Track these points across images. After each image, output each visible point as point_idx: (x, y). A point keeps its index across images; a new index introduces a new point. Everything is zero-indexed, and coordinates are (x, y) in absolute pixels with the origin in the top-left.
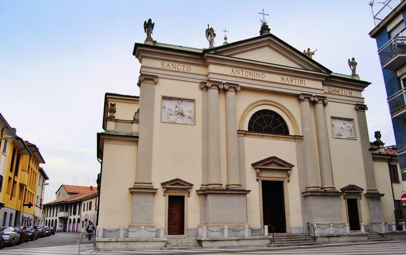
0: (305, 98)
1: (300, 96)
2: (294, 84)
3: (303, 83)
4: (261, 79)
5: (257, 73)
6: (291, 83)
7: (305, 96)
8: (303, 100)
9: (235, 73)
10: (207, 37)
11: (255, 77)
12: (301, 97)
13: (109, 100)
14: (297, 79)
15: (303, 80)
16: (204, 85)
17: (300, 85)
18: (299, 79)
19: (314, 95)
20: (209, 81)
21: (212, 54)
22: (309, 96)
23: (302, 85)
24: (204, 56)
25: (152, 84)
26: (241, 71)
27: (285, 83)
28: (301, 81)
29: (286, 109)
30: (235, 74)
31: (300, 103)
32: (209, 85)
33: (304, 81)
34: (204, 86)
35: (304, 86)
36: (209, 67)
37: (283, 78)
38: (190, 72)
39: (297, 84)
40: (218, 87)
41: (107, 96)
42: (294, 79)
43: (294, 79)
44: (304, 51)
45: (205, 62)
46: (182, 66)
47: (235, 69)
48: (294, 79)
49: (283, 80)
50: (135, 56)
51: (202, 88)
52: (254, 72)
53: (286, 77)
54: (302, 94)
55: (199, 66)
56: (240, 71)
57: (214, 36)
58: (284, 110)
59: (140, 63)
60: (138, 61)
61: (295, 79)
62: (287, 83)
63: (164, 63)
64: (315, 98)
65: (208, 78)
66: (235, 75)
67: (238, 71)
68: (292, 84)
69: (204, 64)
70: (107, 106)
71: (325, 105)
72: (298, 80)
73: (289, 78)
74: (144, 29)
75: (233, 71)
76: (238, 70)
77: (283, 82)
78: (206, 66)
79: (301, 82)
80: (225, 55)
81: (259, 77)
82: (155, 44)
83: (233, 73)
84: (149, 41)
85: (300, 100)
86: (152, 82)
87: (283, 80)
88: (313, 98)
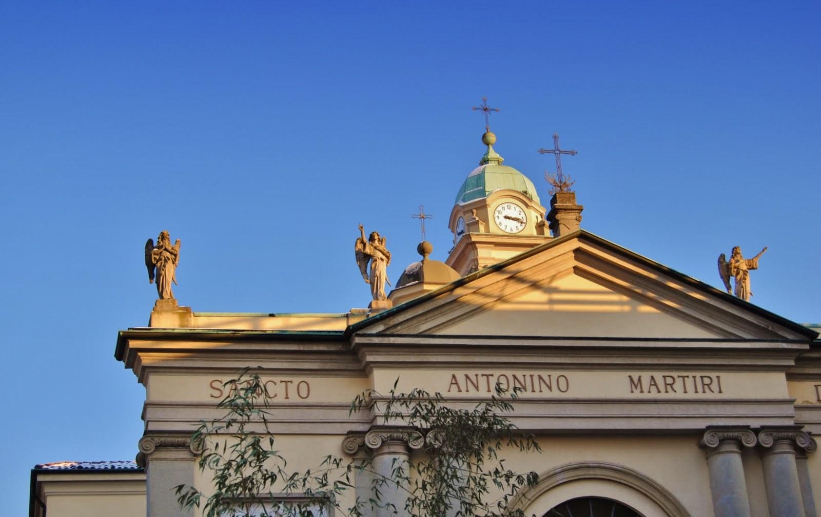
0: (722, 441)
1: (703, 437)
2: (680, 395)
3: (714, 386)
4: (555, 394)
5: (540, 377)
6: (667, 392)
7: (720, 434)
8: (716, 451)
9: (463, 388)
10: (360, 268)
11: (533, 391)
12: (707, 438)
13: (47, 490)
14: (690, 374)
15: (713, 375)
16: (359, 440)
17: (700, 396)
18: (698, 374)
19: (755, 424)
20: (375, 428)
21: (379, 335)
22: (736, 434)
23: (709, 396)
24: (350, 344)
25: (182, 459)
26: (483, 375)
27: (646, 396)
28: (707, 381)
29: (655, 488)
30: (462, 388)
31: (707, 459)
32: (373, 441)
33: (715, 381)
34: (359, 446)
35: (716, 396)
36: (371, 376)
37: (636, 380)
38: (310, 400)
39: (691, 395)
40: (406, 444)
41: (40, 478)
42: (679, 377)
43: (677, 379)
44: (722, 260)
45: (359, 361)
46: (281, 382)
47: (460, 374)
48: (679, 377)
49: (639, 387)
50: (122, 364)
51: (353, 452)
52: (528, 373)
53: (646, 376)
54: (709, 428)
55: (336, 375)
56: (480, 377)
57: (382, 260)
58: (650, 491)
59: (141, 384)
60: (136, 379)
61: (683, 377)
62: (654, 395)
63: (212, 396)
64: (762, 436)
65: (371, 417)
66: (464, 395)
67: (474, 379)
68: (671, 395)
69: (351, 366)
70: (41, 509)
71: (803, 453)
72: (694, 377)
73: (658, 375)
74: (146, 268)
75: (454, 382)
76: (472, 373)
77: (637, 395)
78: (364, 372)
79: (704, 385)
80: (424, 327)
81: (550, 388)
82: (188, 320)
83: (454, 386)
84: (166, 311)
85: (707, 452)
86: (183, 454)
87: (639, 387)
88: (752, 436)
